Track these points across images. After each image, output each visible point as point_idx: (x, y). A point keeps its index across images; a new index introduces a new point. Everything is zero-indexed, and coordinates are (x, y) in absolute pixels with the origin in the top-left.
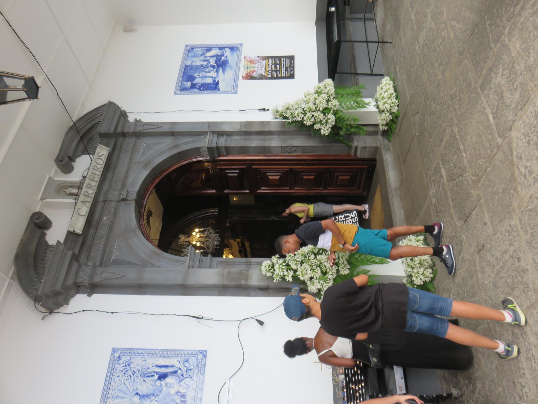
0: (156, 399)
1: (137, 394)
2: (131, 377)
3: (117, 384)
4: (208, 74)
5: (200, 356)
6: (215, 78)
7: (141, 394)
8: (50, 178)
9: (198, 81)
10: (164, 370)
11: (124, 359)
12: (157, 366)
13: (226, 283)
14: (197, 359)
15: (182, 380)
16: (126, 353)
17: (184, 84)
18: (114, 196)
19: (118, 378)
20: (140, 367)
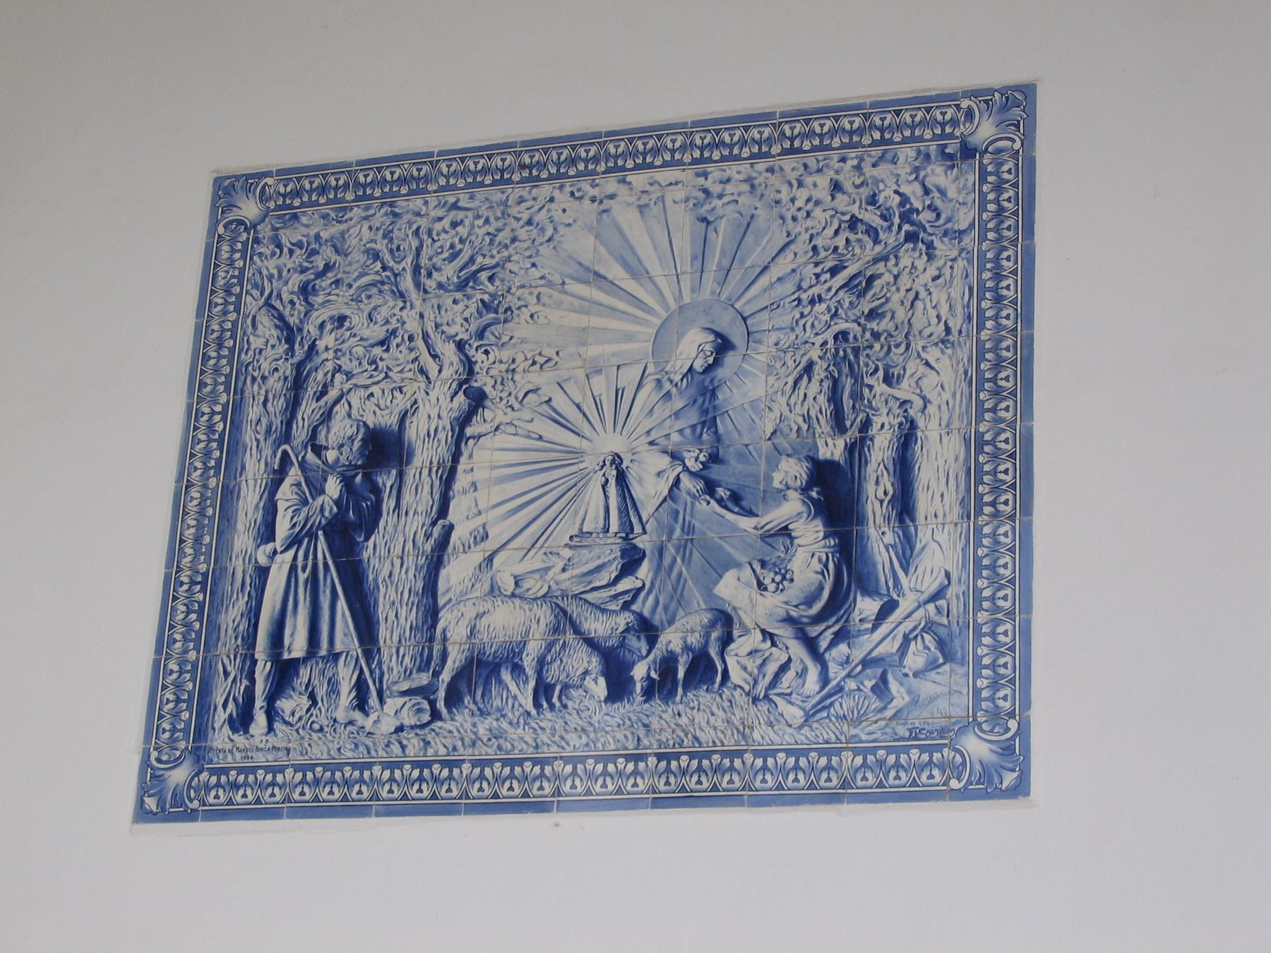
0: (687, 483)
1: (723, 345)
2: (834, 271)
3: (784, 196)
5: (977, 747)
7: (721, 373)
10: (876, 488)
12: (907, 437)
14: (962, 731)
15: (811, 645)
16: (998, 188)
19: (823, 193)
20: (901, 314)
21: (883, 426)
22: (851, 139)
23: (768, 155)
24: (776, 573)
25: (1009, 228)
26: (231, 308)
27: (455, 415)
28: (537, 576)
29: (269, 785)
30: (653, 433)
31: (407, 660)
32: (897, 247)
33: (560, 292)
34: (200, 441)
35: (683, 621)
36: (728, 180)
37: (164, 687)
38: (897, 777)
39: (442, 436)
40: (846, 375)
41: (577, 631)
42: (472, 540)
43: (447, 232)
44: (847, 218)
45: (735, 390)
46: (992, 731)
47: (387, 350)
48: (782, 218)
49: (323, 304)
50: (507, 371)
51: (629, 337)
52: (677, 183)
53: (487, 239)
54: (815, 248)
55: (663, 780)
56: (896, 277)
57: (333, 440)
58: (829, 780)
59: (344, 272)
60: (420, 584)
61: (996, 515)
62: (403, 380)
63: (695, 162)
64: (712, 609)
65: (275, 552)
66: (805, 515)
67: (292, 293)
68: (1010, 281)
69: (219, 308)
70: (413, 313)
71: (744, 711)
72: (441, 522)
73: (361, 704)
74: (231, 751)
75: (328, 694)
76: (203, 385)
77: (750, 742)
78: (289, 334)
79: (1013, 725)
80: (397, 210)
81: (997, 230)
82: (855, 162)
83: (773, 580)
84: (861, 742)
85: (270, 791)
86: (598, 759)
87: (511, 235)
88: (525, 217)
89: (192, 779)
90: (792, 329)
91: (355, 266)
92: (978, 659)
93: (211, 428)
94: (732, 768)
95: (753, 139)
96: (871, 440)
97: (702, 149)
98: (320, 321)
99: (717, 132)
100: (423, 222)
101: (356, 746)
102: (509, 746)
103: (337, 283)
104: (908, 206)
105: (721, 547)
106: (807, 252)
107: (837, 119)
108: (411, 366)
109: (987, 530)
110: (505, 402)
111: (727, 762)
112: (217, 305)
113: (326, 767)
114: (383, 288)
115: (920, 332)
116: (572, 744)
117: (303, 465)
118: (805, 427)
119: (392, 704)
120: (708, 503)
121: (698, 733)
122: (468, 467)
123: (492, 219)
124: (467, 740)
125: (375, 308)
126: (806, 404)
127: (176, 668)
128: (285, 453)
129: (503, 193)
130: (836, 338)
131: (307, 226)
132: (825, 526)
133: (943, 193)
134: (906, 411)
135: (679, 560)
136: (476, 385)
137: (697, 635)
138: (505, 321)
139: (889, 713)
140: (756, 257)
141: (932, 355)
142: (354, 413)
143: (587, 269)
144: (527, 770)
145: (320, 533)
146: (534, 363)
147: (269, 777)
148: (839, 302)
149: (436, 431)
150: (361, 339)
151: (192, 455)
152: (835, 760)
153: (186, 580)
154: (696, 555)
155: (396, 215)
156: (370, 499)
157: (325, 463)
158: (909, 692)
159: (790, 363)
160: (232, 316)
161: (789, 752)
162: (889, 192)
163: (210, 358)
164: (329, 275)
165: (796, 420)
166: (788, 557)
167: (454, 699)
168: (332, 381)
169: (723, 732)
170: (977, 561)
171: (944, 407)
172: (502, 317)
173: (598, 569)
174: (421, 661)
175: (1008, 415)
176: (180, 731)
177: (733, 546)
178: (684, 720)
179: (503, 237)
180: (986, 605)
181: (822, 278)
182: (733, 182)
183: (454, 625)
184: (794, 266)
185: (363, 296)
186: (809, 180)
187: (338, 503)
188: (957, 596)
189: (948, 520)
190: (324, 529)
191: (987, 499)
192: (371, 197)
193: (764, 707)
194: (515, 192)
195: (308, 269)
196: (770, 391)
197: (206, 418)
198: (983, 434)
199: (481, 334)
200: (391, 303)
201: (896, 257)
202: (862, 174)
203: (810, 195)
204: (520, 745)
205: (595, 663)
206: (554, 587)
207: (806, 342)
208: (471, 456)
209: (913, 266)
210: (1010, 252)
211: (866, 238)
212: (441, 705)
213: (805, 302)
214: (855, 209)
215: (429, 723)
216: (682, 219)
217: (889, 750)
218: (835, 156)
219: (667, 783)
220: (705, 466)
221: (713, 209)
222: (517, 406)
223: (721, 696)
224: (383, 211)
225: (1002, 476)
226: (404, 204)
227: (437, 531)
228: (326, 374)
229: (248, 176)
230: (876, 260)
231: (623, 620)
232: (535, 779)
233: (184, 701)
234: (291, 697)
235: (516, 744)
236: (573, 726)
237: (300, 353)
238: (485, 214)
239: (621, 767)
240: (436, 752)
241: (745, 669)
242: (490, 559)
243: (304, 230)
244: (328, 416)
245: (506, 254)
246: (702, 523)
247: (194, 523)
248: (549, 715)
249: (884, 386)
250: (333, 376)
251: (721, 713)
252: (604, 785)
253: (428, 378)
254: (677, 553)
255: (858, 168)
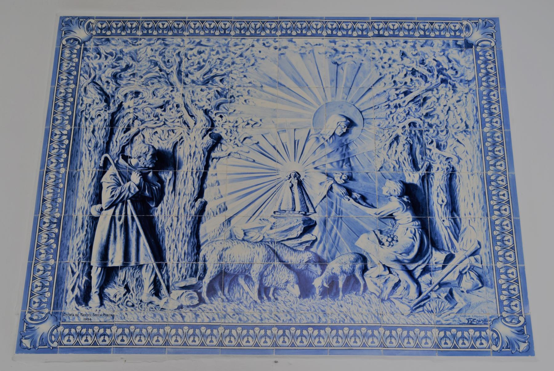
0: (336, 188)
1: (351, 124)
2: (406, 93)
3: (377, 56)
7: (350, 137)
11: (465, 61)
12: (451, 175)
14: (495, 320)
15: (410, 273)
19: (397, 55)
20: (442, 117)
21: (438, 169)
22: (409, 33)
23: (366, 36)
24: (388, 237)
25: (493, 81)
26: (72, 82)
27: (205, 146)
28: (256, 231)
29: (101, 335)
30: (316, 163)
31: (183, 270)
32: (437, 86)
33: (260, 90)
34: (54, 149)
35: (340, 258)
36: (347, 46)
37: (34, 278)
38: (463, 343)
39: (198, 156)
41: (281, 261)
42: (218, 210)
43: (196, 56)
44: (410, 69)
45: (358, 146)
46: (511, 322)
47: (165, 111)
48: (377, 66)
49: (126, 85)
50: (233, 127)
51: (300, 116)
52: (320, 45)
53: (219, 61)
54: (395, 82)
55: (335, 340)
56: (438, 99)
57: (134, 153)
58: (426, 343)
59: (138, 70)
60: (189, 231)
61: (501, 215)
62: (174, 126)
63: (328, 36)
64: (355, 253)
65: (102, 209)
66: (401, 209)
67: (108, 77)
68: (496, 106)
69: (64, 81)
70: (178, 93)
72: (199, 200)
73: (157, 292)
74: (77, 315)
75: (137, 286)
76: (55, 120)
77: (382, 322)
78: (107, 98)
79: (522, 319)
80: (167, 42)
81: (487, 81)
82: (412, 44)
83: (387, 241)
84: (442, 324)
85: (102, 338)
86: (297, 328)
87: (232, 61)
88: (239, 53)
89: (53, 330)
90: (387, 119)
91: (143, 68)
92: (499, 286)
93: (61, 142)
94: (373, 335)
95: (358, 28)
96: (433, 175)
97: (332, 30)
98: (124, 93)
99: (340, 23)
100: (183, 51)
101: (155, 315)
102: (246, 319)
103: (134, 75)
104: (441, 67)
105: (357, 222)
106: (391, 83)
107: (401, 23)
108: (179, 120)
109: (497, 222)
110: (232, 142)
111: (370, 332)
112: (62, 79)
113: (136, 327)
114: (160, 80)
115: (453, 126)
116: (282, 319)
117: (117, 165)
118: (397, 166)
119: (175, 293)
120: (349, 200)
121: (353, 316)
122: (214, 173)
123: (220, 52)
124: (220, 314)
125: (156, 89)
126: (397, 155)
127: (41, 268)
128: (106, 159)
129: (226, 40)
130: (410, 125)
131: (115, 45)
132: (412, 215)
133: (458, 62)
134: (449, 162)
135: (335, 227)
136: (216, 132)
137: (348, 266)
138: (231, 102)
139: (456, 310)
140: (365, 83)
141: (460, 137)
142: (146, 140)
143: (275, 81)
144: (257, 332)
145: (129, 201)
146: (248, 124)
147: (102, 331)
148: (410, 108)
149: (194, 153)
150: (149, 104)
151: (50, 156)
152: (429, 333)
153: (47, 221)
154: (344, 226)
155: (166, 45)
156: (157, 185)
157: (130, 165)
158: (465, 300)
159: (387, 135)
160: (73, 86)
161: (404, 328)
162: (431, 59)
163: (59, 106)
164: (129, 70)
165: (392, 162)
166: (394, 229)
167: (211, 291)
168: (133, 123)
169: (366, 316)
170: (494, 237)
171: (469, 162)
172: (229, 100)
173: (291, 229)
174: (192, 271)
175: (502, 168)
176: (45, 303)
177: (364, 222)
178: (344, 309)
179: (228, 61)
180: (501, 259)
181: (400, 96)
182: (349, 47)
183: (210, 254)
184: (385, 89)
185: (149, 83)
186: (389, 50)
187: (138, 186)
188: (485, 254)
189: (477, 216)
190: (130, 199)
191: (496, 207)
192: (151, 35)
193: (388, 304)
194: (233, 41)
195: (116, 66)
196: (378, 148)
197: (58, 136)
198: (490, 176)
199: (218, 107)
200: (166, 88)
201: (437, 89)
202: (416, 50)
203: (392, 57)
204: (251, 319)
205: (292, 277)
206: (266, 237)
207: (394, 126)
208: (215, 167)
209: (446, 95)
210: (495, 92)
211: (420, 79)
212: (204, 295)
213: (392, 107)
214: (414, 66)
215: (197, 305)
217: (458, 329)
218: (402, 40)
219: (337, 342)
220: (346, 182)
221: (340, 59)
222: (240, 144)
223: (364, 297)
224: (159, 42)
225: (502, 197)
226: (170, 40)
227: (198, 204)
228: (129, 120)
229: (79, 18)
230: (427, 90)
231: (306, 256)
232: (261, 337)
233: (47, 287)
234: (114, 287)
235: (249, 318)
236: (282, 309)
237: (113, 108)
238: (217, 49)
239: (310, 332)
240: (203, 320)
241: (376, 284)
242: (229, 220)
243: (114, 47)
244: (131, 141)
245: (229, 69)
246: (346, 209)
247: (52, 191)
248: (267, 303)
249: (437, 150)
250: (133, 121)
251: (364, 306)
252: (302, 342)
253: (188, 127)
254: (334, 223)
255: (414, 46)
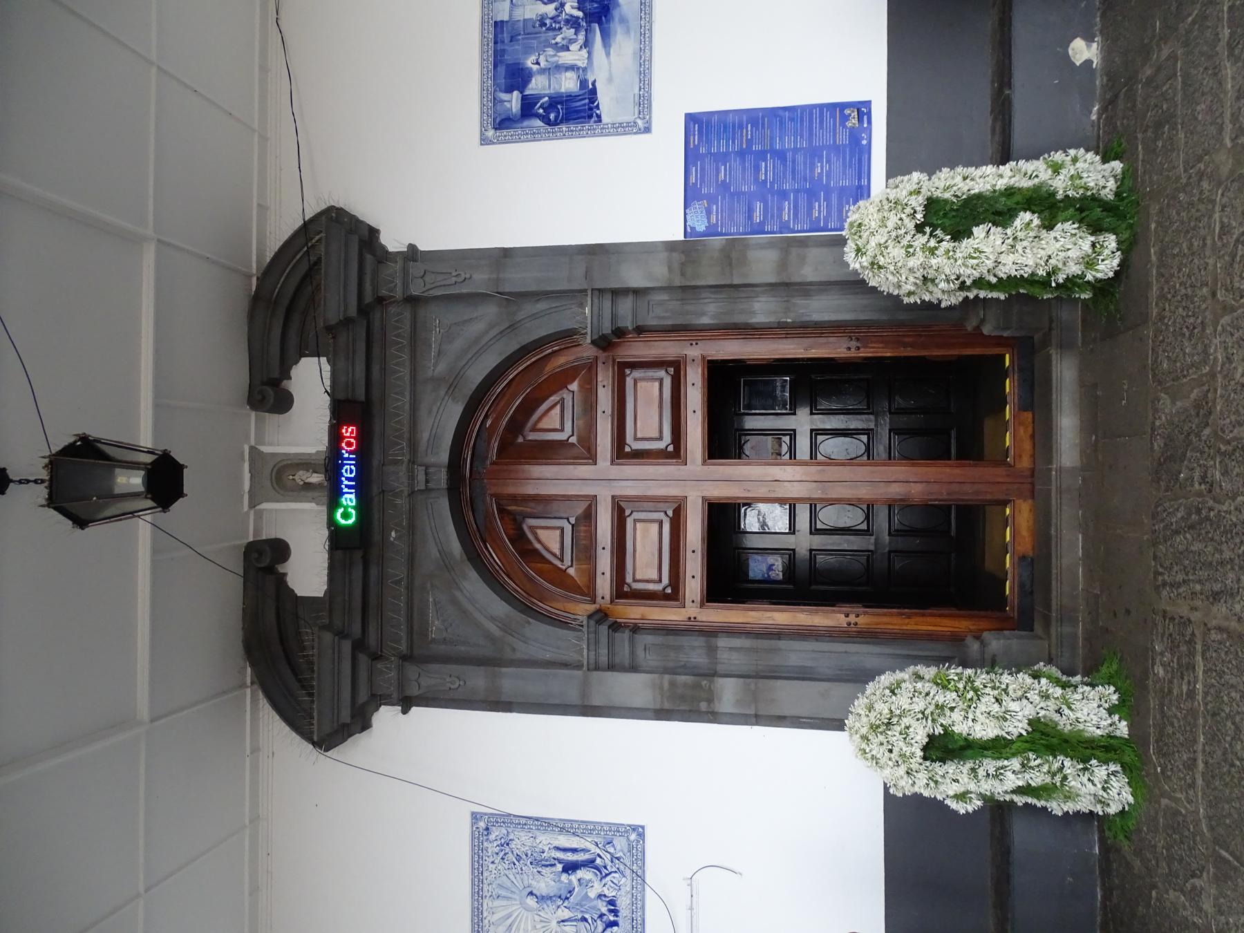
1: (531, 893)
4: (566, 58)
5: (633, 837)
6: (585, 70)
8: (252, 448)
9: (538, 85)
12: (558, 849)
13: (667, 706)
15: (607, 875)
17: (502, 101)
18: (397, 478)
40: (542, 863)
71: (622, 892)
140: (509, 884)
205: (609, 930)
216: (497, 903)
231: (599, 922)
